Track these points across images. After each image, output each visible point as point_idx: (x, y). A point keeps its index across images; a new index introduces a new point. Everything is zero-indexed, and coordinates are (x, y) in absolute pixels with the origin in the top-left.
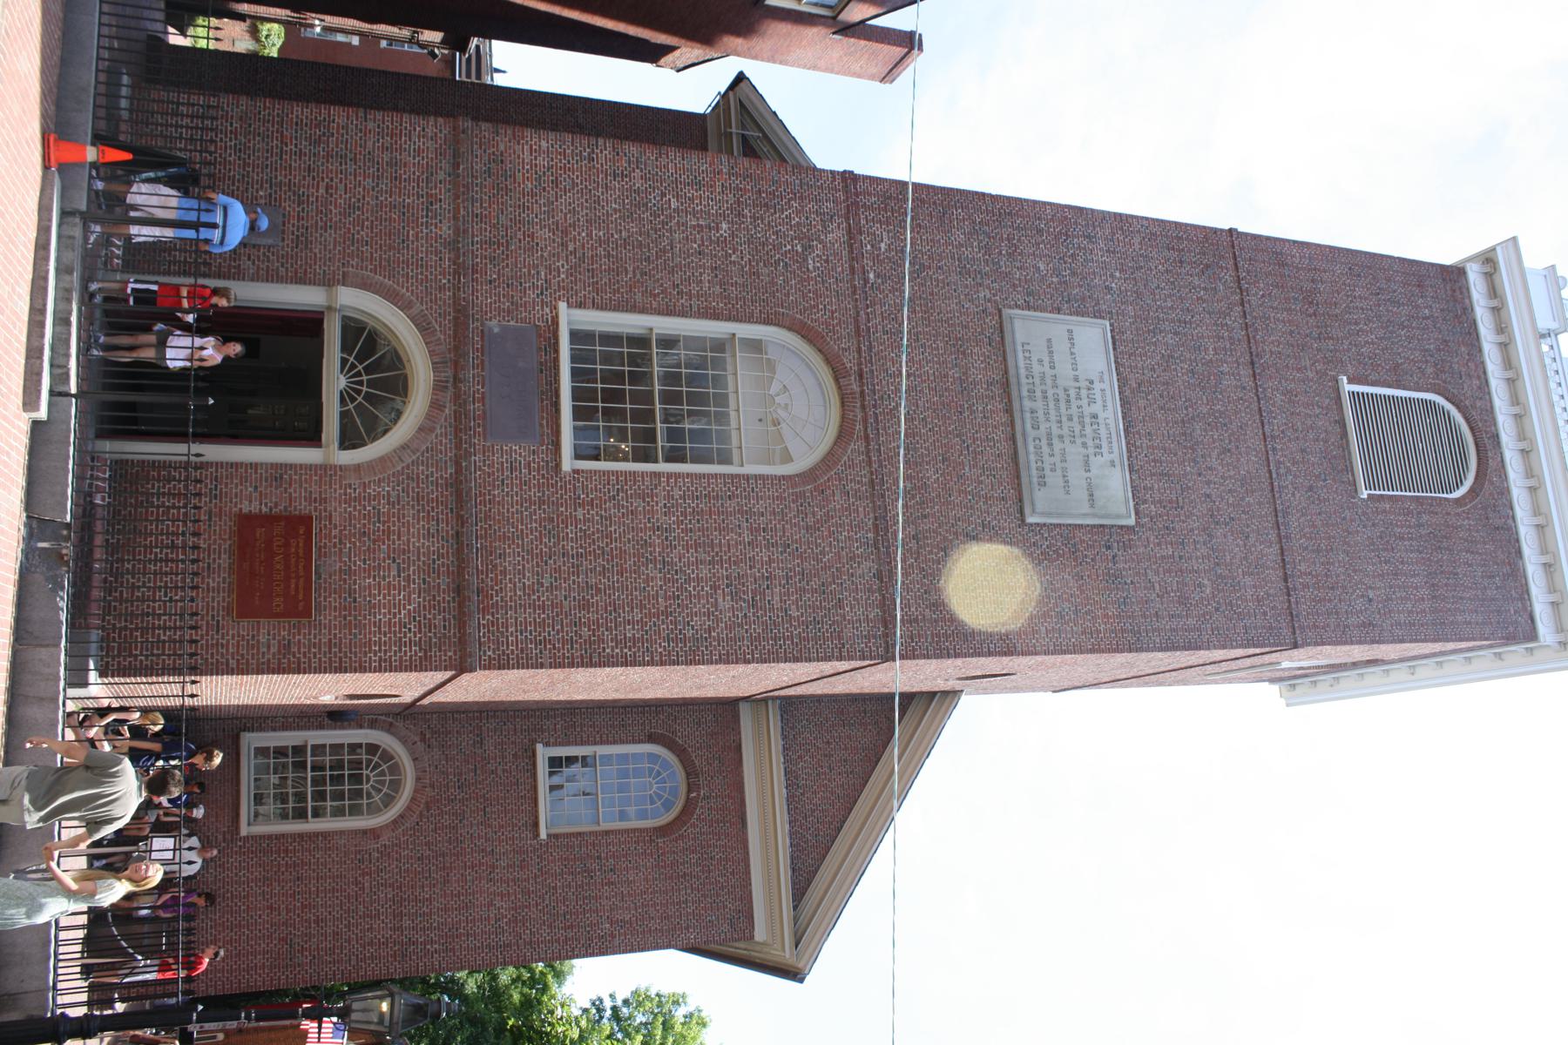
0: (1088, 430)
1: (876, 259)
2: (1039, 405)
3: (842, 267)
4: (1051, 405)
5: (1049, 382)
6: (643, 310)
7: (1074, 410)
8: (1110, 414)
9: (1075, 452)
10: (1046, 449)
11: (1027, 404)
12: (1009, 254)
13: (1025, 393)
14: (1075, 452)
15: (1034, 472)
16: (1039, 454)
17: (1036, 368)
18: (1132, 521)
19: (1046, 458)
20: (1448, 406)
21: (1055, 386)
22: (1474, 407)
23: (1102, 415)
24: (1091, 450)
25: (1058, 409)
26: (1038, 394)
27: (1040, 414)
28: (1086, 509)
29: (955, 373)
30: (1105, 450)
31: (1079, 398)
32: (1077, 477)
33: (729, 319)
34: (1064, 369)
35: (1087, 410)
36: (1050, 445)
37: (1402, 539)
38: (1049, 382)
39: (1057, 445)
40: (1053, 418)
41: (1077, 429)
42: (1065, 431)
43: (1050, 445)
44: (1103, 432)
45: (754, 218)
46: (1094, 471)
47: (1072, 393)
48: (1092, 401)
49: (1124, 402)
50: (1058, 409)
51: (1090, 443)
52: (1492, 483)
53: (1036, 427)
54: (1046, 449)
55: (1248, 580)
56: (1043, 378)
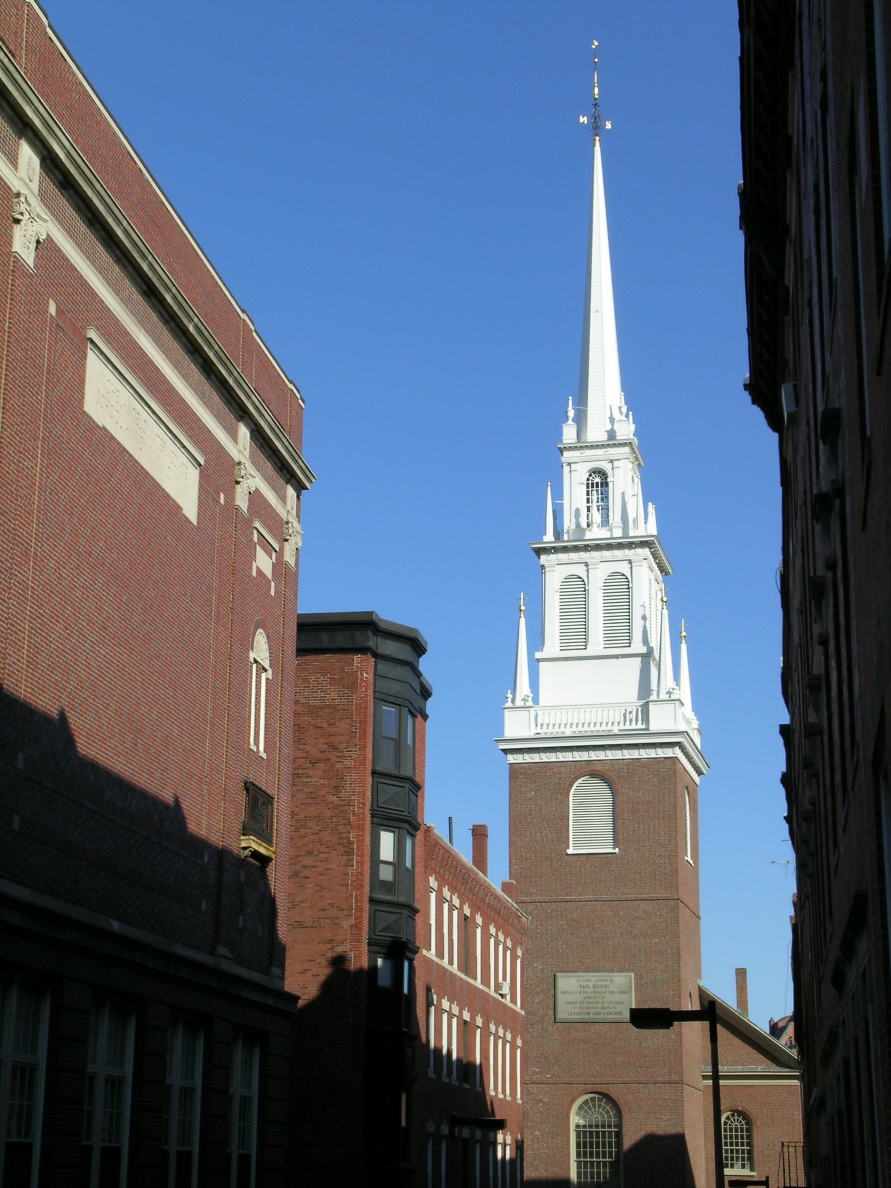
0: (599, 990)
1: (541, 1073)
2: (592, 1011)
3: (547, 1087)
4: (590, 1005)
5: (582, 1005)
6: (569, 1165)
7: (591, 995)
8: (594, 978)
9: (608, 998)
10: (608, 1010)
11: (592, 1016)
12: (534, 1015)
13: (587, 1016)
14: (608, 998)
15: (616, 1016)
16: (610, 1013)
17: (577, 1010)
18: (633, 975)
19: (611, 1010)
20: (574, 787)
21: (583, 1003)
22: (574, 773)
23: (593, 983)
24: (607, 990)
25: (592, 1003)
26: (587, 1010)
27: (595, 1011)
28: (628, 995)
29: (582, 1046)
30: (605, 983)
31: (587, 993)
32: (618, 997)
33: (569, 1133)
34: (577, 997)
35: (592, 989)
36: (606, 1008)
37: (634, 831)
38: (582, 1005)
39: (606, 1005)
40: (595, 1005)
41: (599, 995)
42: (600, 1000)
43: (606, 1008)
44: (599, 983)
45: (532, 1121)
46: (614, 990)
47: (586, 995)
48: (588, 986)
49: (587, 970)
50: (592, 1003)
51: (604, 990)
52: (608, 770)
53: (600, 1014)
54: (608, 1010)
55: (653, 919)
56: (581, 1008)
